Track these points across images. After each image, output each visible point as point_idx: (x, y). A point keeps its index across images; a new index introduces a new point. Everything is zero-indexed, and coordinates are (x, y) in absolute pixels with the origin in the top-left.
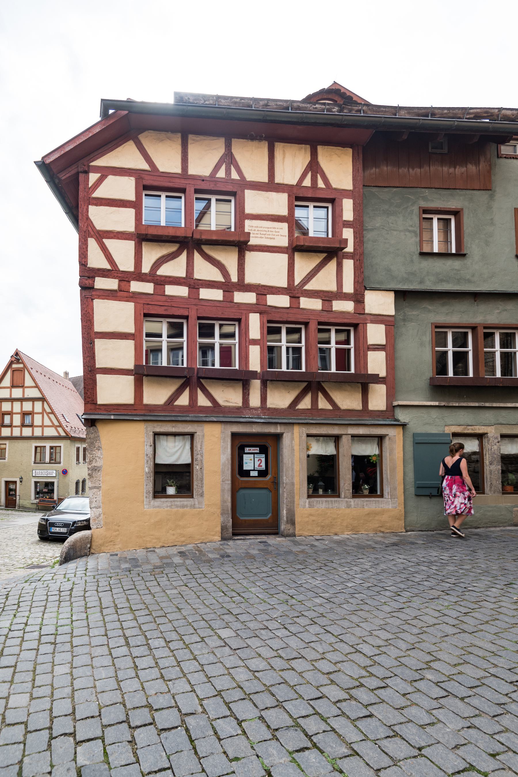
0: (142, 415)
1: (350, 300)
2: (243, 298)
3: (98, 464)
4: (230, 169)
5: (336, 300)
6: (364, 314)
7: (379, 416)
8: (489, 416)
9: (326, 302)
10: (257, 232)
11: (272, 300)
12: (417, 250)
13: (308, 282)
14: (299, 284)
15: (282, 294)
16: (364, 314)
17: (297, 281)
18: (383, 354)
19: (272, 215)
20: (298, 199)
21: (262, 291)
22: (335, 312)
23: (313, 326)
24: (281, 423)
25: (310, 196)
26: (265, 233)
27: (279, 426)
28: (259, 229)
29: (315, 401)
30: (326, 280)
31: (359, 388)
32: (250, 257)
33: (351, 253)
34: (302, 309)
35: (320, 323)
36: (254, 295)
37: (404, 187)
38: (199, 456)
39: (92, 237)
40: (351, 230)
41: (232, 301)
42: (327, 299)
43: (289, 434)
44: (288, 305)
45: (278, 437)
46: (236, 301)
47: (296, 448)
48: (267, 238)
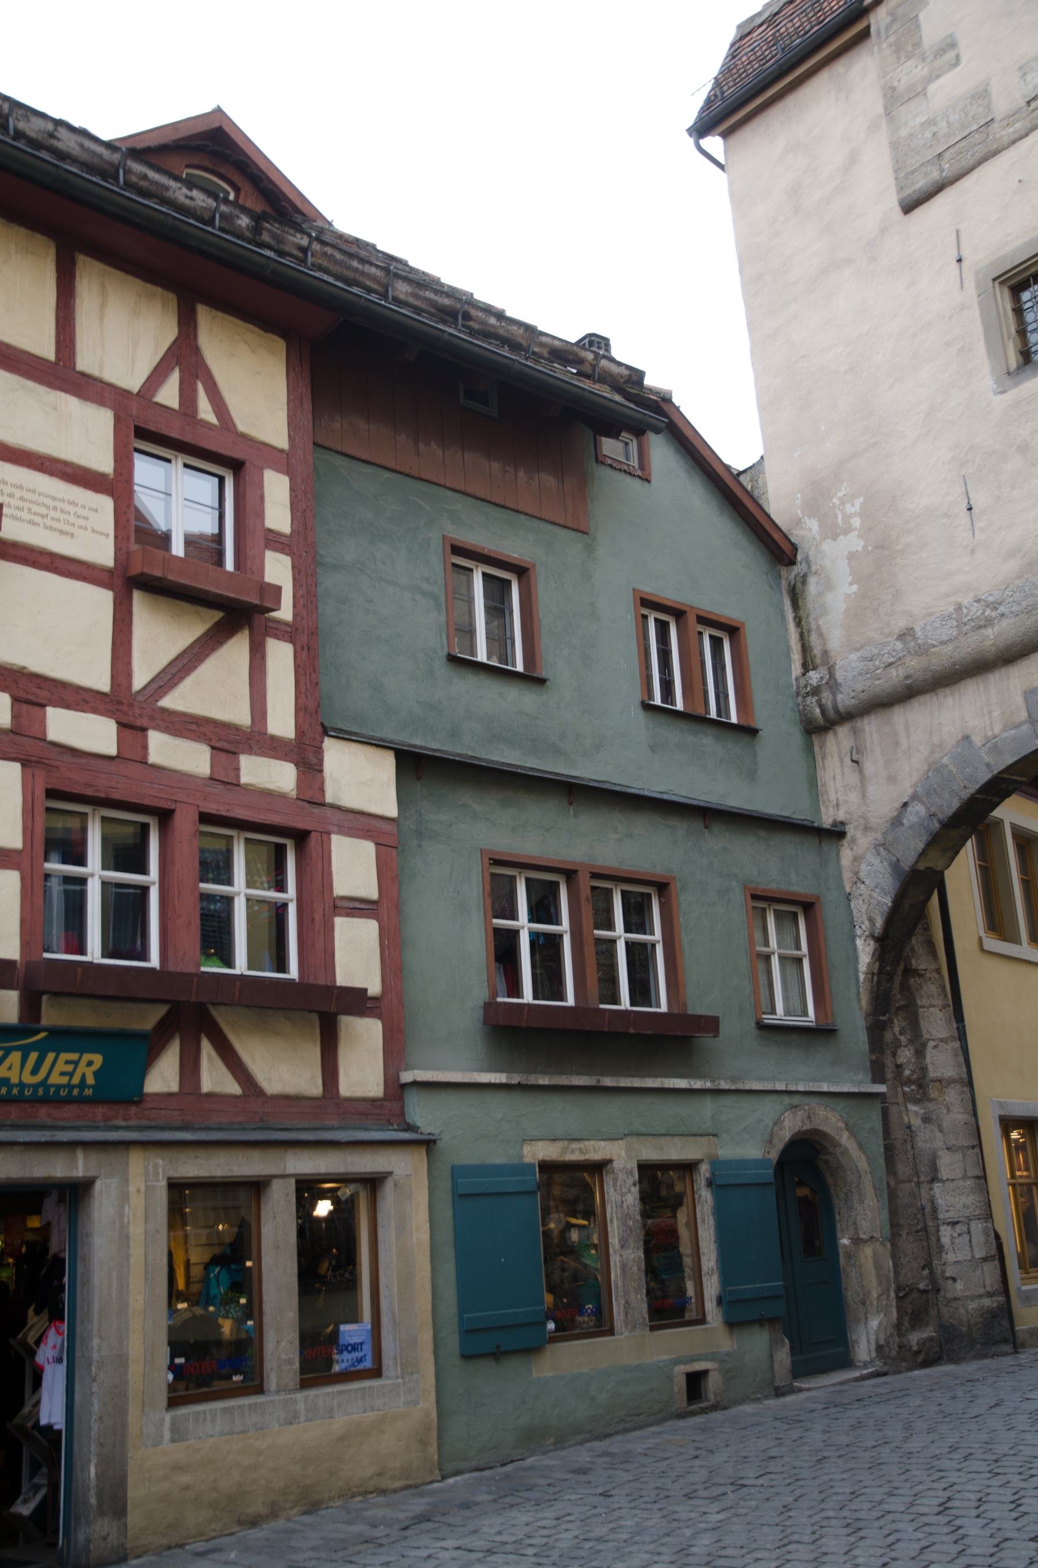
5: (250, 754)
6: (323, 804)
7: (365, 1114)
8: (610, 1112)
9: (223, 755)
10: (20, 504)
11: (63, 726)
12: (442, 647)
14: (144, 688)
20: (142, 433)
24: (86, 1145)
27: (80, 1155)
29: (190, 1068)
30: (219, 689)
35: (206, 818)
37: (407, 475)
43: (115, 1182)
48: (51, 528)
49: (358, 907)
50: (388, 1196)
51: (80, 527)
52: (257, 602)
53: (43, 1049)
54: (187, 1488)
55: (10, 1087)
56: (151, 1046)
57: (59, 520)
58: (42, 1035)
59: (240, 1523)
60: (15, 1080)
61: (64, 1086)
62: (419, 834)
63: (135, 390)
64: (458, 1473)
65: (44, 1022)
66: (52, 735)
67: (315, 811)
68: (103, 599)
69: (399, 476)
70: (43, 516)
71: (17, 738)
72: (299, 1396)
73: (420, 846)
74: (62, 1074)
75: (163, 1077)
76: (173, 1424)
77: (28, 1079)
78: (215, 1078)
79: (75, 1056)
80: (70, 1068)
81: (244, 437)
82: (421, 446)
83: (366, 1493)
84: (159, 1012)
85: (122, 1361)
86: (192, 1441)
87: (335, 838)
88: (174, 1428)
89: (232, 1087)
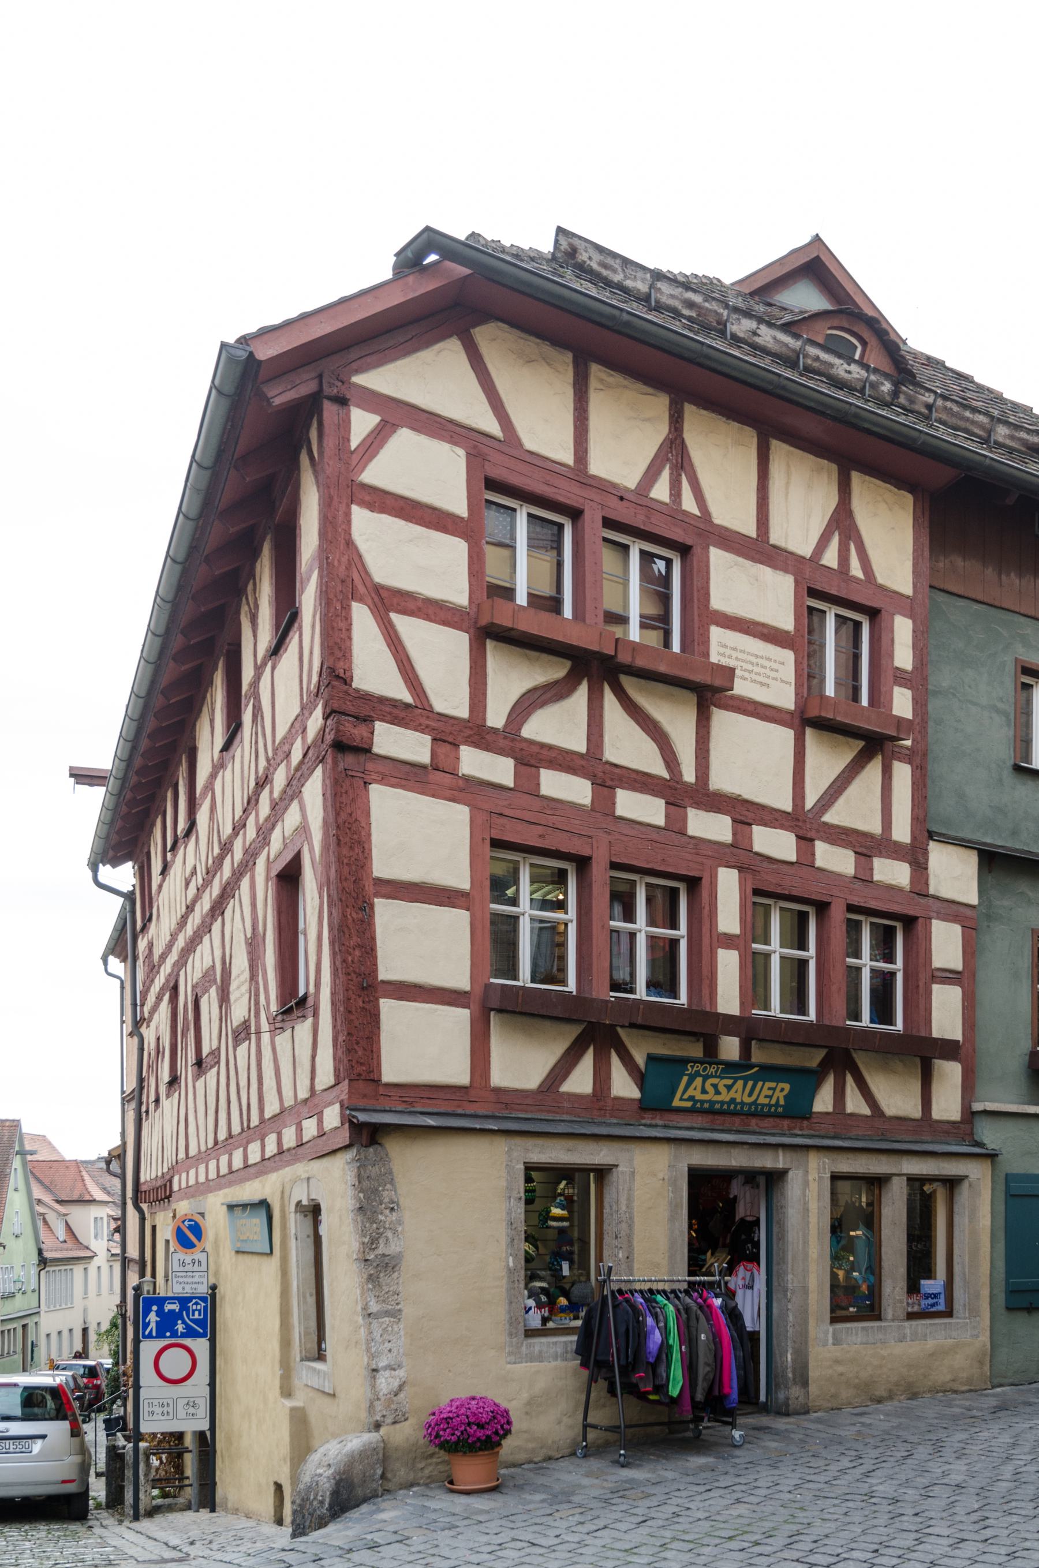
0: (486, 1117)
2: (710, 827)
3: (393, 1248)
4: (680, 483)
15: (782, 827)
16: (927, 896)
19: (763, 625)
23: (838, 914)
27: (780, 1152)
28: (741, 656)
34: (818, 868)
36: (726, 821)
37: (991, 605)
38: (624, 1226)
41: (683, 832)
44: (793, 858)
47: (813, 1206)
49: (949, 977)
50: (963, 1194)
51: (773, 679)
52: (895, 734)
53: (756, 1079)
54: (841, 1374)
55: (736, 1104)
56: (816, 1077)
57: (759, 674)
58: (756, 1069)
59: (872, 1400)
60: (739, 1100)
61: (766, 1105)
63: (808, 556)
64: (1001, 1385)
65: (754, 1060)
67: (922, 901)
68: (787, 735)
69: (984, 606)
70: (750, 672)
72: (907, 1324)
74: (766, 1096)
75: (823, 1102)
76: (834, 1334)
77: (747, 1100)
78: (855, 1103)
79: (773, 1085)
80: (770, 1093)
81: (882, 588)
82: (1004, 577)
83: (945, 1391)
84: (821, 1053)
85: (805, 1290)
86: (845, 1346)
87: (934, 922)
88: (835, 1337)
89: (866, 1111)
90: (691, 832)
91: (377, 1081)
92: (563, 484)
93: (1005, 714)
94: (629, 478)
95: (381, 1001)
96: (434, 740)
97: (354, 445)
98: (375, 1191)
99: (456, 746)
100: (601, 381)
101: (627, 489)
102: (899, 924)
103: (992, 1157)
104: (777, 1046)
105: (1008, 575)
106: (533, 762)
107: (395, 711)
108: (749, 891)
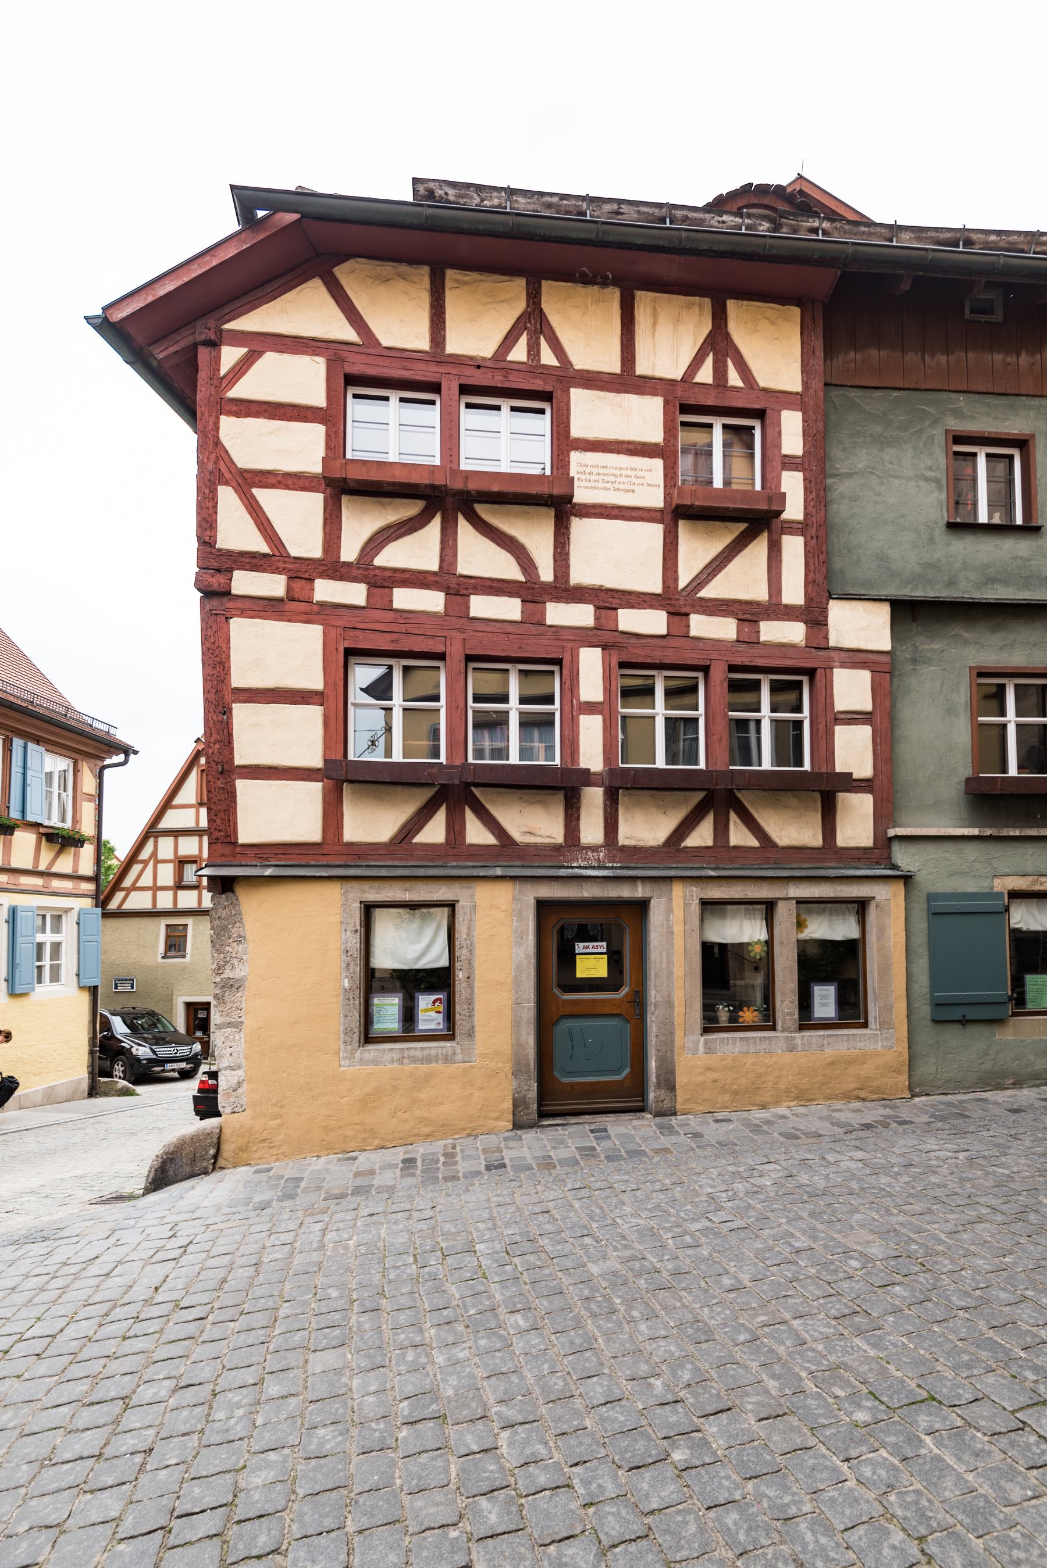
1: (796, 619)
4: (539, 344)
6: (827, 648)
9: (747, 624)
13: (707, 583)
15: (651, 607)
17: (684, 579)
18: (866, 731)
19: (629, 442)
20: (685, 409)
21: (607, 600)
22: (767, 645)
23: (719, 674)
25: (712, 404)
26: (613, 479)
28: (601, 471)
30: (745, 578)
31: (815, 801)
32: (578, 526)
33: (799, 522)
34: (694, 638)
35: (733, 668)
36: (589, 609)
39: (227, 483)
40: (799, 476)
42: (749, 617)
45: (642, 907)
46: (549, 621)
62: (914, 661)
66: (622, 627)
71: (599, 632)
73: (914, 670)
90: (549, 622)
91: (234, 843)
92: (422, 366)
93: (937, 481)
94: (485, 348)
95: (237, 781)
96: (290, 578)
97: (223, 372)
98: (224, 929)
99: (312, 580)
100: (457, 281)
101: (484, 359)
102: (799, 677)
103: (907, 879)
104: (646, 792)
105: (933, 356)
106: (386, 584)
107: (255, 561)
108: (614, 664)
